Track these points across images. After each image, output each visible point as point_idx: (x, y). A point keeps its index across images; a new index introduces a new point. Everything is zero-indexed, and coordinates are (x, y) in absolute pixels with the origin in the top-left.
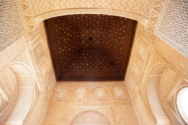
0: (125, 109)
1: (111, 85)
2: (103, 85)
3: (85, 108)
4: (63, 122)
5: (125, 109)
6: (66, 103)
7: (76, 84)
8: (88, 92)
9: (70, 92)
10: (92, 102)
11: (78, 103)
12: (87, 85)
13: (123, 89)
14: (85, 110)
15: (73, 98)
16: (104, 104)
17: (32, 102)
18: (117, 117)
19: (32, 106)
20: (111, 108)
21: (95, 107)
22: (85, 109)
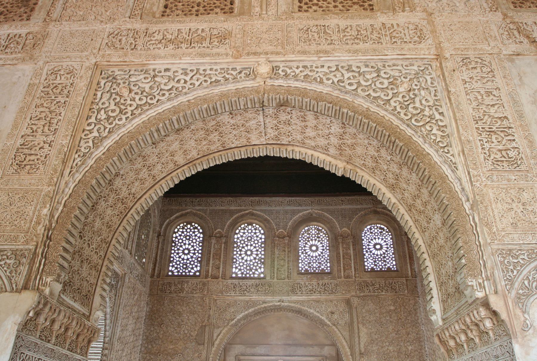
0: (392, 308)
1: (360, 210)
2: (327, 211)
3: (264, 302)
4: (201, 347)
5: (392, 308)
6: (204, 284)
7: (233, 208)
8: (273, 242)
9: (213, 241)
10: (287, 280)
11: (242, 282)
12: (270, 212)
13: (395, 229)
14: (263, 306)
15: (225, 263)
16: (325, 289)
17: (105, 320)
18: (362, 334)
19: (108, 328)
20: (348, 302)
21: (295, 298)
22: (266, 305)
